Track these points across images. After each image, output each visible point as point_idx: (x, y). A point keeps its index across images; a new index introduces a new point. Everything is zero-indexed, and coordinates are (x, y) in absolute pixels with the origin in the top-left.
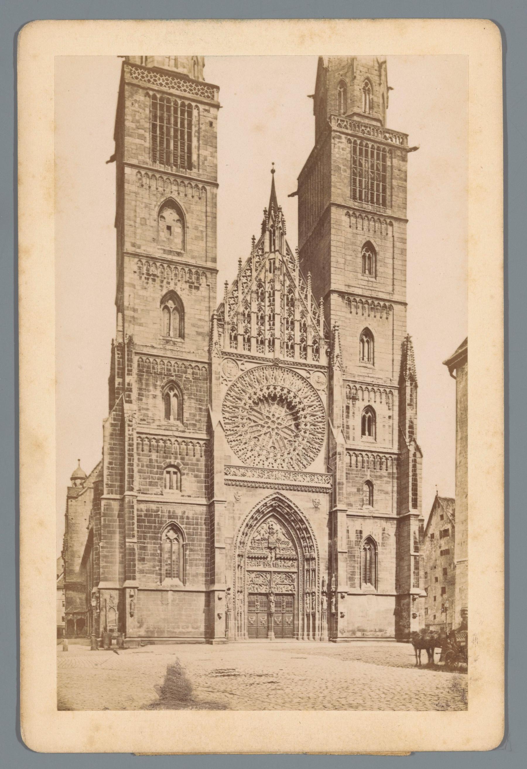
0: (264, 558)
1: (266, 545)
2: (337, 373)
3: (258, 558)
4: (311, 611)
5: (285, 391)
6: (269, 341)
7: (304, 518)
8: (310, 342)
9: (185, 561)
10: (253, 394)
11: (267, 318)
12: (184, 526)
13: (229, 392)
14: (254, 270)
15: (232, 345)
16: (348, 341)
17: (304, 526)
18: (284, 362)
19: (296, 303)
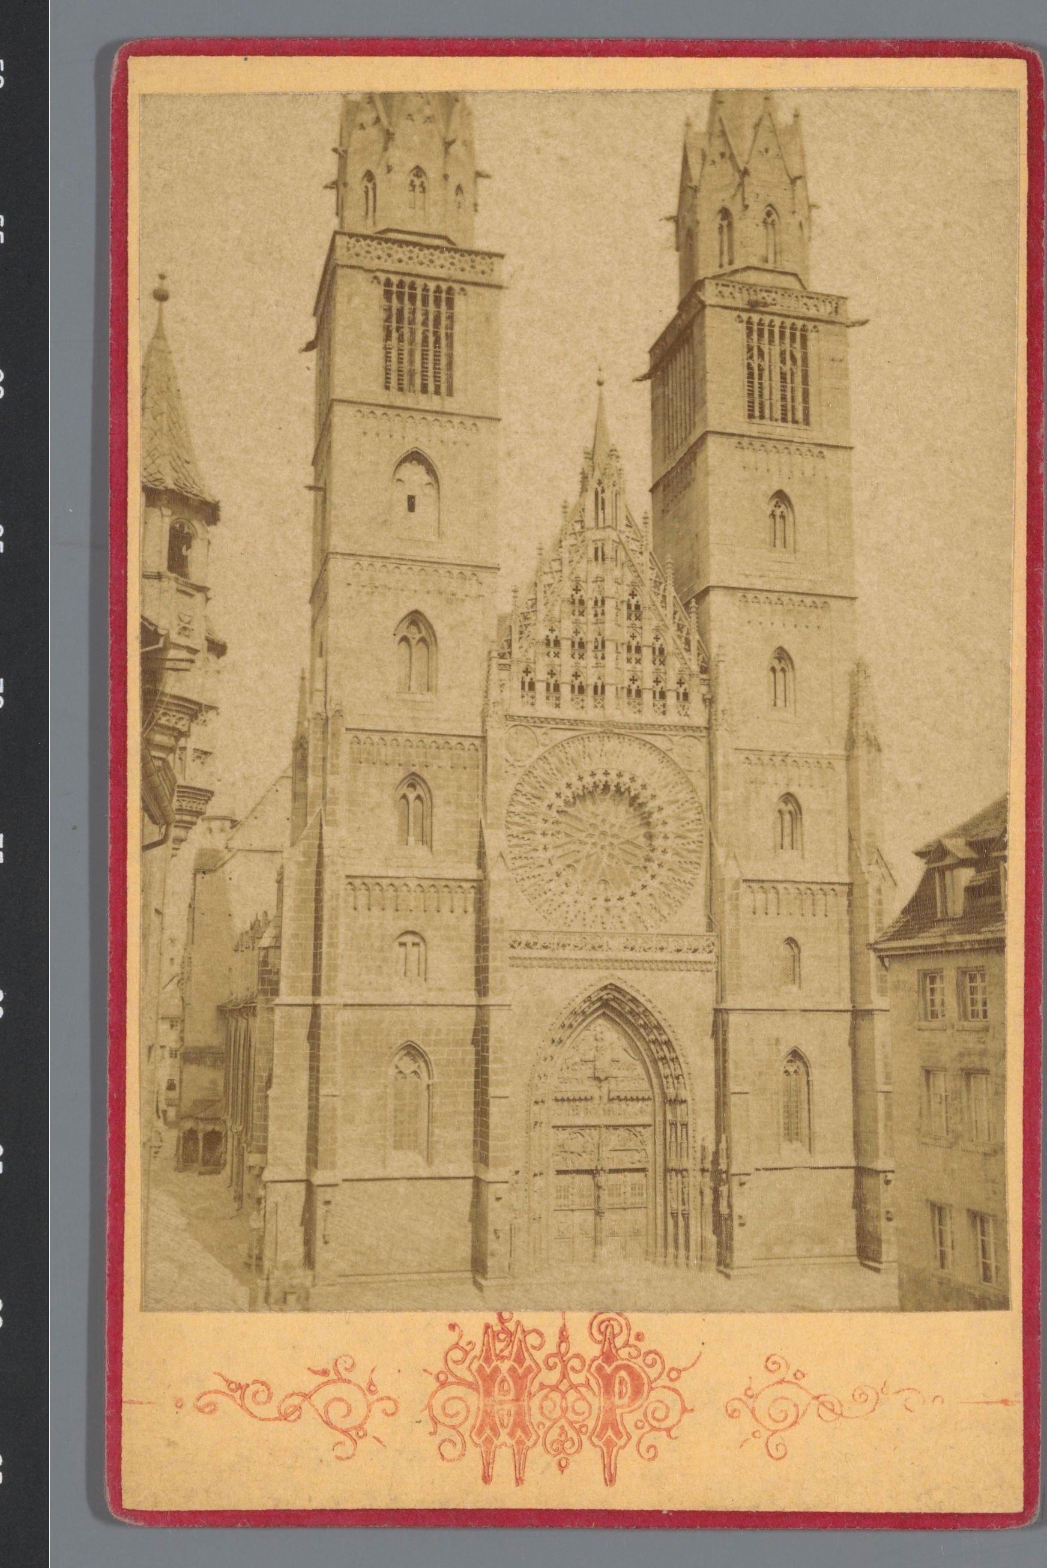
0: (586, 1099)
1: (590, 1073)
2: (721, 733)
3: (574, 1100)
4: (681, 1208)
5: (626, 779)
6: (596, 687)
7: (663, 1024)
8: (671, 683)
9: (431, 1119)
10: (563, 787)
11: (590, 647)
12: (431, 1048)
13: (519, 787)
14: (566, 562)
15: (525, 699)
16: (742, 677)
17: (664, 1038)
18: (623, 726)
19: (646, 614)
